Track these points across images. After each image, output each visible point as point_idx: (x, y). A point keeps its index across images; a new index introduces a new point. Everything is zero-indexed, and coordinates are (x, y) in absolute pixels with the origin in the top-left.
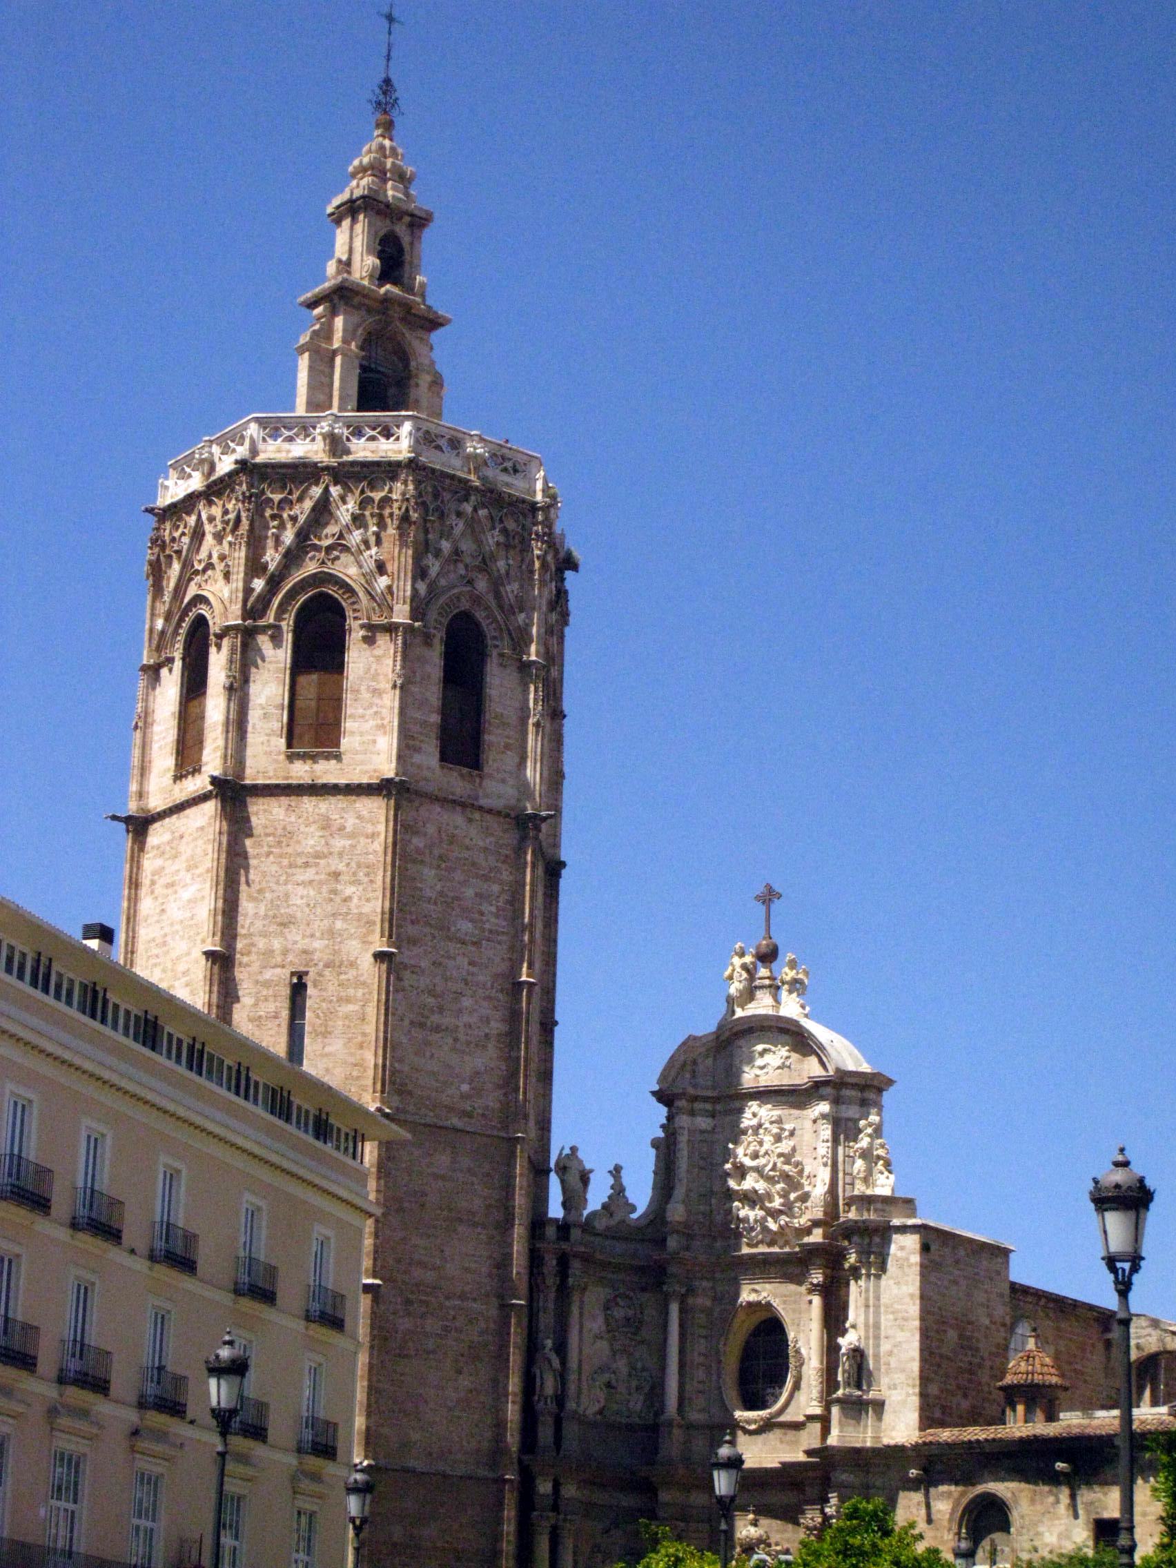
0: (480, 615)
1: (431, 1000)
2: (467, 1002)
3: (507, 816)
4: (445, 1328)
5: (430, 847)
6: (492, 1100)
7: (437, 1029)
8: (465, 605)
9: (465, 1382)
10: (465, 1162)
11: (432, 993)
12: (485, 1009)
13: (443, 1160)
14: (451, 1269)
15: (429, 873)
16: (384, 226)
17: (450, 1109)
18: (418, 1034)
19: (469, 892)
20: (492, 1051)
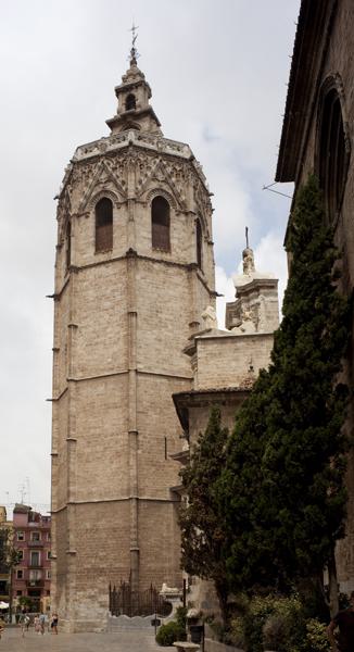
0: (109, 197)
1: (94, 335)
2: (108, 330)
3: (122, 258)
4: (106, 448)
5: (91, 284)
6: (122, 360)
7: (97, 343)
8: (102, 196)
9: (114, 466)
10: (112, 386)
11: (94, 332)
12: (118, 329)
13: (101, 389)
14: (106, 426)
15: (91, 292)
16: (126, 96)
17: (103, 370)
18: (90, 348)
19: (108, 291)
20: (121, 343)
